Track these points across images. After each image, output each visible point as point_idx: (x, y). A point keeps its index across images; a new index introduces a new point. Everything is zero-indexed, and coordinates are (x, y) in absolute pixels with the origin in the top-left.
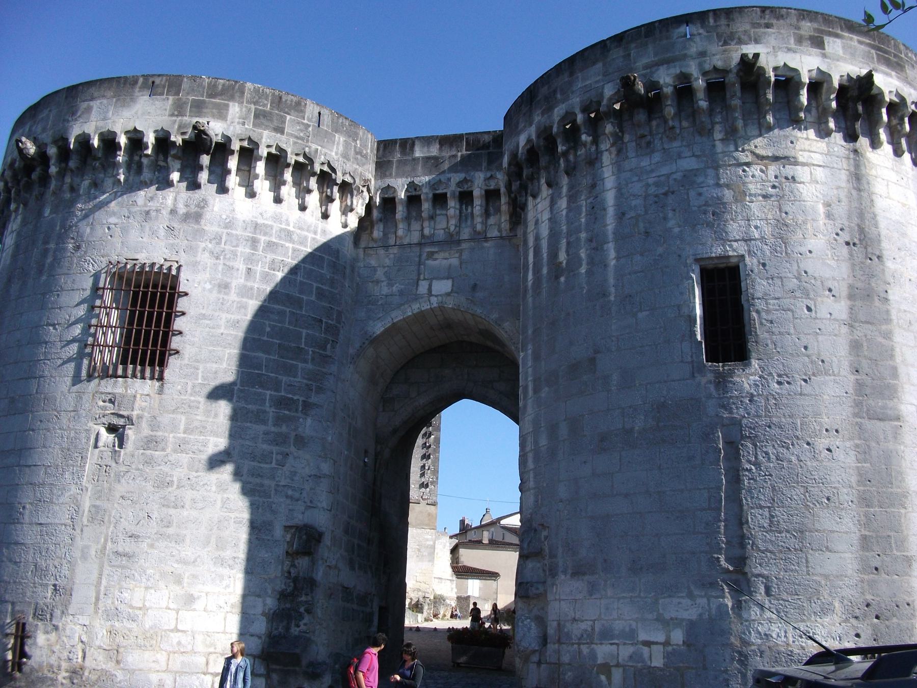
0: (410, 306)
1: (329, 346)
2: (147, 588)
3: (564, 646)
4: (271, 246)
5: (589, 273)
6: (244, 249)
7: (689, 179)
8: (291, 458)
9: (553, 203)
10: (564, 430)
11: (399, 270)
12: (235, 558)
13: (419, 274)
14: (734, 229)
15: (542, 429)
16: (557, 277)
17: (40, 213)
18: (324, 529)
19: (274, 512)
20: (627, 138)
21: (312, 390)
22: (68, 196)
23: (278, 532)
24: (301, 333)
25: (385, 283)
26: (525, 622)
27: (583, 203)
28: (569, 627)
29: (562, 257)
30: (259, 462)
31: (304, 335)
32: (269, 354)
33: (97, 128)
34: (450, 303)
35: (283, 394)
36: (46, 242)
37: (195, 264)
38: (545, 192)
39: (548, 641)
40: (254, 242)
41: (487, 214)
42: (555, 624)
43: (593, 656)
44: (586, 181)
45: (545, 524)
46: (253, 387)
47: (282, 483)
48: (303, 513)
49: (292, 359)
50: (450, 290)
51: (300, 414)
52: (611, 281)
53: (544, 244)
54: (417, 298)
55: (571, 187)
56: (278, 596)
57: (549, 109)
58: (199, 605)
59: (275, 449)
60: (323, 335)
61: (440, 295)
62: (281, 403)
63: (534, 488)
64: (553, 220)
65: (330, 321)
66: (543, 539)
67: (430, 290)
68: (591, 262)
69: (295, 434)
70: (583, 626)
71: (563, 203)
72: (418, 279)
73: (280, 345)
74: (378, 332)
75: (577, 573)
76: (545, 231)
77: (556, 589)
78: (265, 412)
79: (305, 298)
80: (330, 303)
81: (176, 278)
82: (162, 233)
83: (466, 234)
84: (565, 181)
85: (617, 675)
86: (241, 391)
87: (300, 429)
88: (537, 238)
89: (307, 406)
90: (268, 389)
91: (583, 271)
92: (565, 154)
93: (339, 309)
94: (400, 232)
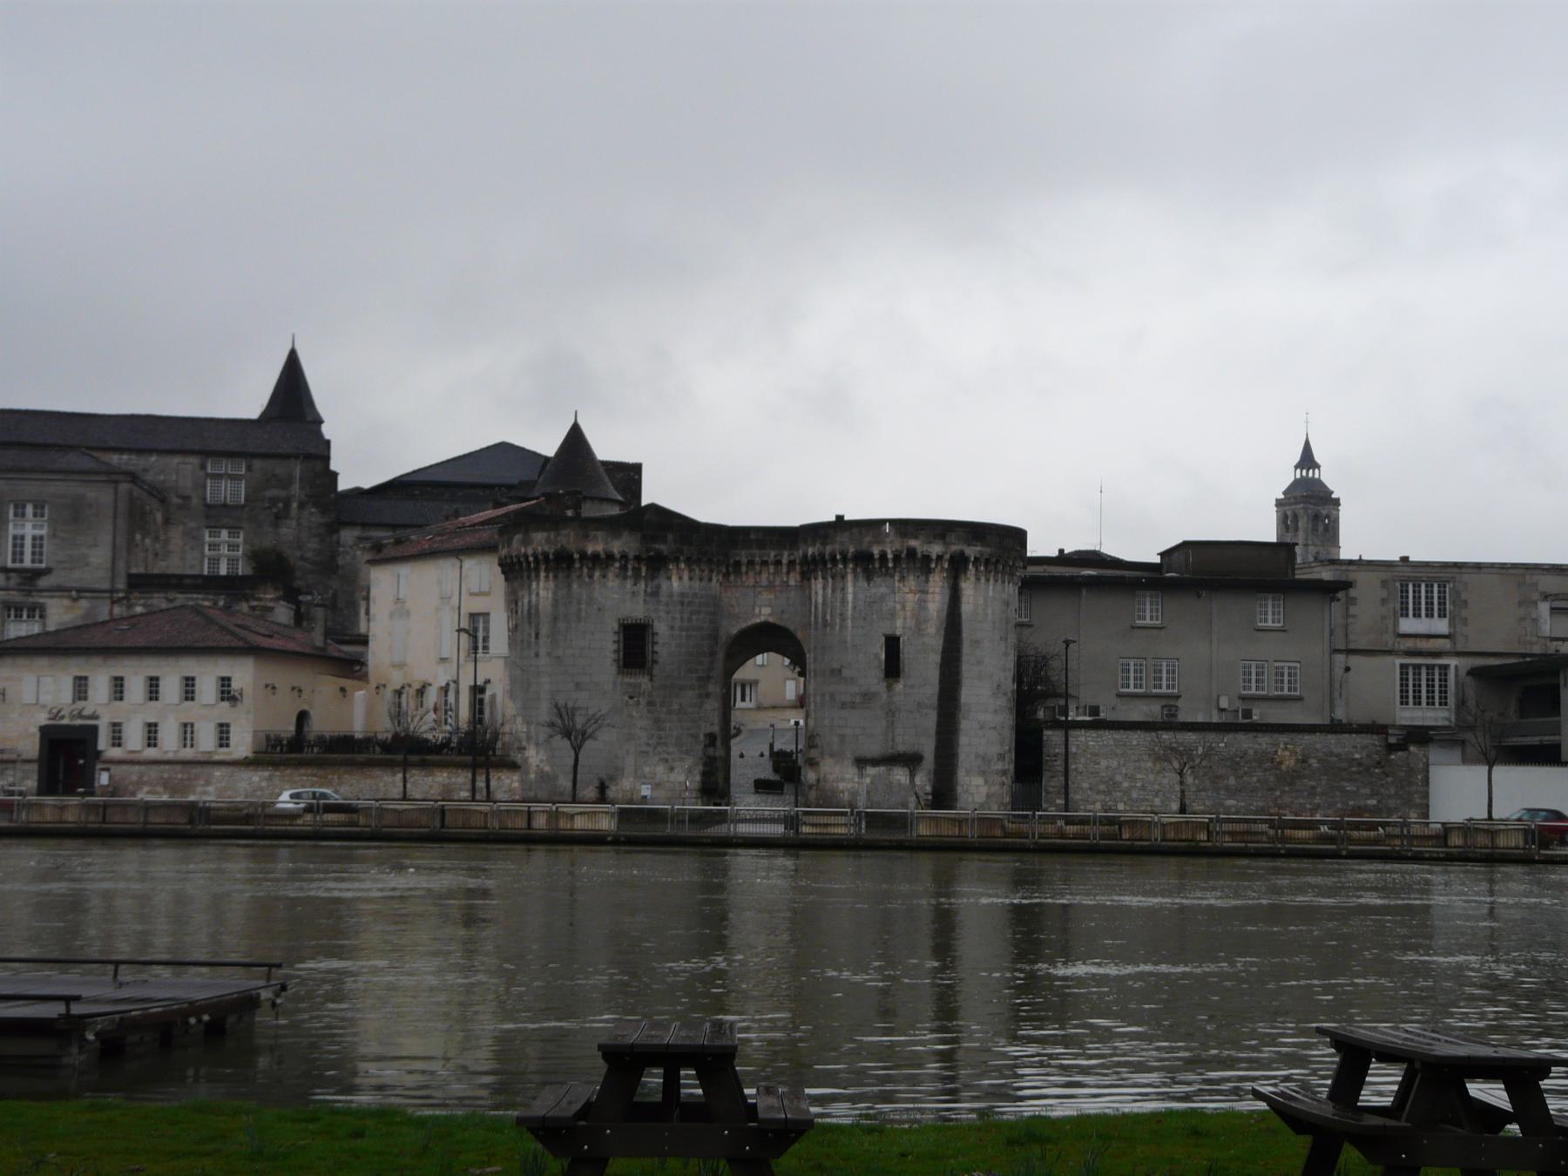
4: (690, 603)
5: (840, 630)
6: (679, 607)
7: (883, 597)
9: (824, 588)
10: (827, 698)
14: (899, 623)
17: (569, 586)
20: (859, 570)
22: (587, 579)
23: (702, 737)
27: (839, 595)
28: (828, 776)
29: (828, 617)
33: (604, 550)
34: (771, 620)
37: (659, 617)
38: (820, 580)
40: (682, 603)
41: (788, 573)
43: (838, 787)
44: (840, 585)
52: (849, 637)
53: (820, 606)
54: (754, 616)
55: (834, 585)
57: (824, 544)
62: (699, 679)
64: (824, 597)
68: (841, 627)
71: (830, 591)
75: (832, 755)
76: (820, 600)
81: (652, 626)
82: (642, 602)
83: (777, 583)
84: (830, 580)
85: (846, 794)
88: (816, 601)
89: (709, 677)
92: (831, 569)
94: (744, 579)
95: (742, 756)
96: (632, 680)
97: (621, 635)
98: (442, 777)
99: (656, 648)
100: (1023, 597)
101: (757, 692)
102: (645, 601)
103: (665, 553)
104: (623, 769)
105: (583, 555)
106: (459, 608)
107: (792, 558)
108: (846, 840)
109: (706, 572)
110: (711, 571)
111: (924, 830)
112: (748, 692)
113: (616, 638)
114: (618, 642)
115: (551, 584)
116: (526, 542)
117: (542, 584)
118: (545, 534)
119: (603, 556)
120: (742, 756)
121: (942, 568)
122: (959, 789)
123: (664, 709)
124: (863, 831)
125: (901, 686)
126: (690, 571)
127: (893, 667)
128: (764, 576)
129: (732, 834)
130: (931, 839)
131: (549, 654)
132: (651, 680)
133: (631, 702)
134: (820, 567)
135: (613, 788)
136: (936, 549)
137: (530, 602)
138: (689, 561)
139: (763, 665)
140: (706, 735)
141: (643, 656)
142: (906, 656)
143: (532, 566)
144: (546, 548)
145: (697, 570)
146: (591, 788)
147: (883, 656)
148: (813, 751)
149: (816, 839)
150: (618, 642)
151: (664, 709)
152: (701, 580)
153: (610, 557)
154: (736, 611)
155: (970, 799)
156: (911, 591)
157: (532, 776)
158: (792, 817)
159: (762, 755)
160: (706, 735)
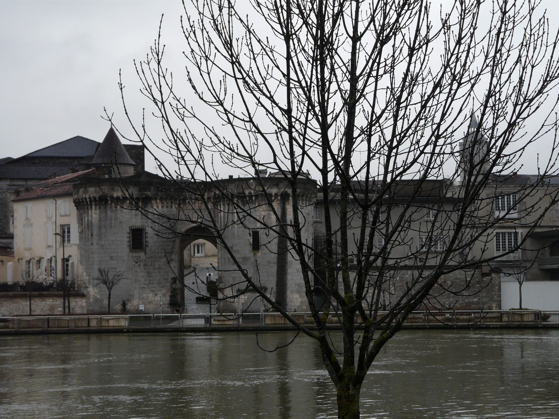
2: (148, 294)
17: (106, 212)
20: (239, 201)
22: (114, 209)
23: (170, 280)
33: (122, 195)
36: (111, 220)
38: (222, 206)
53: (222, 218)
58: (158, 295)
82: (140, 219)
84: (226, 206)
88: (220, 216)
89: (172, 252)
96: (137, 255)
97: (131, 234)
98: (49, 302)
99: (147, 239)
100: (318, 209)
102: (141, 218)
103: (150, 196)
104: (133, 296)
105: (112, 197)
106: (56, 222)
107: (209, 196)
108: (233, 327)
109: (170, 204)
110: (172, 203)
111: (268, 321)
113: (128, 236)
114: (130, 237)
115: (98, 211)
116: (85, 192)
117: (93, 211)
118: (94, 188)
119: (121, 198)
121: (278, 199)
122: (288, 300)
123: (152, 267)
124: (241, 322)
125: (260, 254)
126: (162, 203)
127: (256, 246)
128: (197, 204)
129: (181, 326)
130: (271, 326)
131: (98, 244)
132: (145, 254)
133: (136, 264)
134: (222, 200)
135: (129, 305)
136: (274, 191)
137: (88, 220)
138: (161, 199)
140: (172, 279)
141: (142, 244)
142: (262, 240)
143: (89, 203)
144: (95, 195)
145: (165, 203)
146: (119, 305)
147: (252, 240)
148: (221, 284)
149: (219, 328)
150: (130, 237)
151: (152, 267)
152: (167, 207)
153: (125, 198)
155: (293, 304)
156: (263, 210)
157: (92, 300)
158: (208, 317)
160: (172, 279)
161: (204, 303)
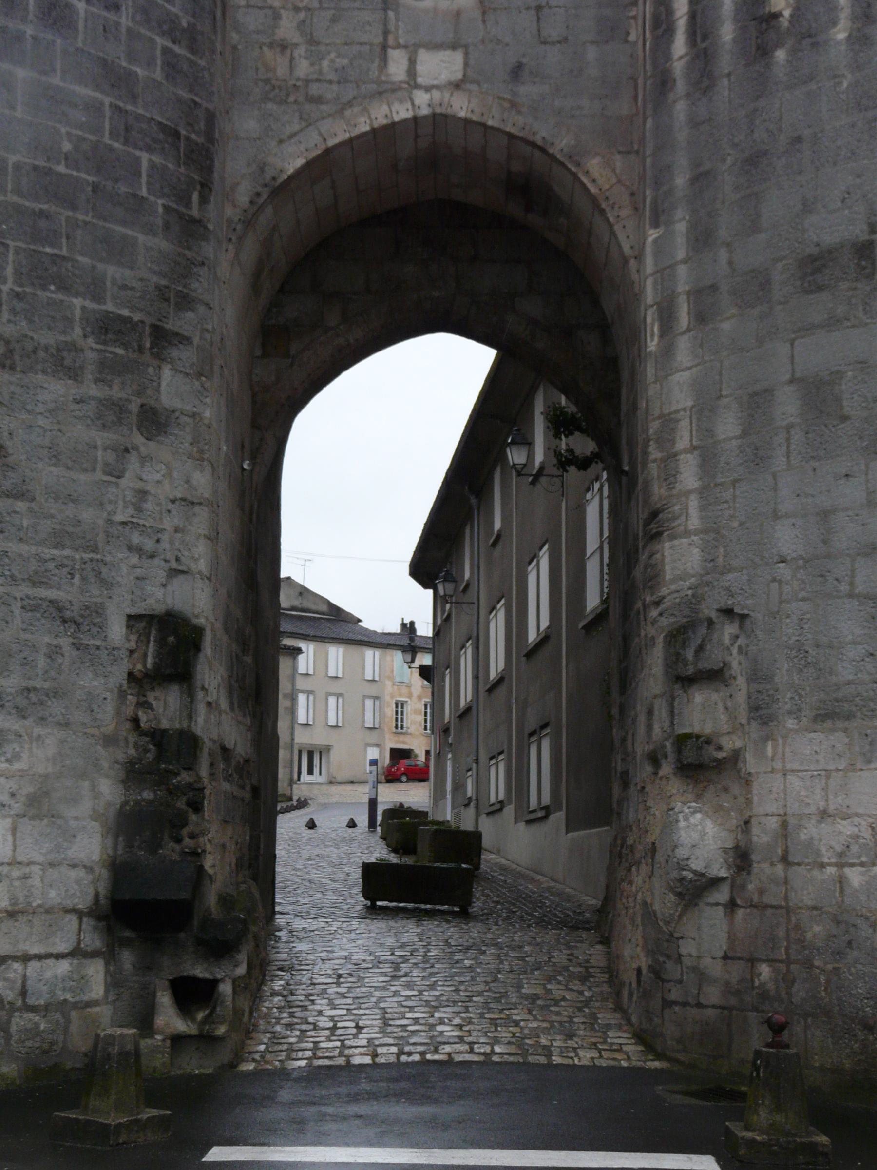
0: (366, 110)
1: (195, 197)
3: (801, 870)
8: (133, 457)
11: (334, 20)
12: (28, 690)
13: (386, 33)
15: (725, 401)
16: (764, 52)
18: (202, 621)
19: (107, 584)
21: (167, 300)
23: (117, 630)
24: (138, 160)
25: (301, 51)
26: (692, 820)
28: (810, 830)
30: (68, 468)
31: (145, 165)
32: (74, 208)
35: (110, 307)
39: (754, 857)
42: (773, 823)
45: (737, 610)
46: (44, 288)
47: (120, 518)
48: (164, 586)
49: (124, 223)
50: (459, 76)
51: (147, 357)
56: (122, 775)
59: (101, 437)
60: (182, 169)
61: (437, 87)
63: (705, 531)
65: (194, 136)
66: (727, 641)
67: (412, 72)
69: (139, 401)
70: (846, 828)
72: (384, 47)
73: (96, 188)
74: (291, 171)
77: (775, 748)
78: (74, 348)
79: (139, 70)
80: (191, 91)
86: (18, 296)
87: (149, 392)
90: (77, 295)
91: (841, 36)
93: (210, 106)
95: (408, 110)
101: (328, 762)
112: (316, 761)
120: (408, 110)
139: (337, 726)
148: (699, 696)
154: (303, 68)
159: (352, 824)
161: (430, 914)
